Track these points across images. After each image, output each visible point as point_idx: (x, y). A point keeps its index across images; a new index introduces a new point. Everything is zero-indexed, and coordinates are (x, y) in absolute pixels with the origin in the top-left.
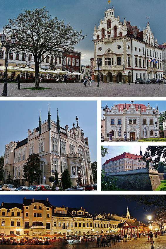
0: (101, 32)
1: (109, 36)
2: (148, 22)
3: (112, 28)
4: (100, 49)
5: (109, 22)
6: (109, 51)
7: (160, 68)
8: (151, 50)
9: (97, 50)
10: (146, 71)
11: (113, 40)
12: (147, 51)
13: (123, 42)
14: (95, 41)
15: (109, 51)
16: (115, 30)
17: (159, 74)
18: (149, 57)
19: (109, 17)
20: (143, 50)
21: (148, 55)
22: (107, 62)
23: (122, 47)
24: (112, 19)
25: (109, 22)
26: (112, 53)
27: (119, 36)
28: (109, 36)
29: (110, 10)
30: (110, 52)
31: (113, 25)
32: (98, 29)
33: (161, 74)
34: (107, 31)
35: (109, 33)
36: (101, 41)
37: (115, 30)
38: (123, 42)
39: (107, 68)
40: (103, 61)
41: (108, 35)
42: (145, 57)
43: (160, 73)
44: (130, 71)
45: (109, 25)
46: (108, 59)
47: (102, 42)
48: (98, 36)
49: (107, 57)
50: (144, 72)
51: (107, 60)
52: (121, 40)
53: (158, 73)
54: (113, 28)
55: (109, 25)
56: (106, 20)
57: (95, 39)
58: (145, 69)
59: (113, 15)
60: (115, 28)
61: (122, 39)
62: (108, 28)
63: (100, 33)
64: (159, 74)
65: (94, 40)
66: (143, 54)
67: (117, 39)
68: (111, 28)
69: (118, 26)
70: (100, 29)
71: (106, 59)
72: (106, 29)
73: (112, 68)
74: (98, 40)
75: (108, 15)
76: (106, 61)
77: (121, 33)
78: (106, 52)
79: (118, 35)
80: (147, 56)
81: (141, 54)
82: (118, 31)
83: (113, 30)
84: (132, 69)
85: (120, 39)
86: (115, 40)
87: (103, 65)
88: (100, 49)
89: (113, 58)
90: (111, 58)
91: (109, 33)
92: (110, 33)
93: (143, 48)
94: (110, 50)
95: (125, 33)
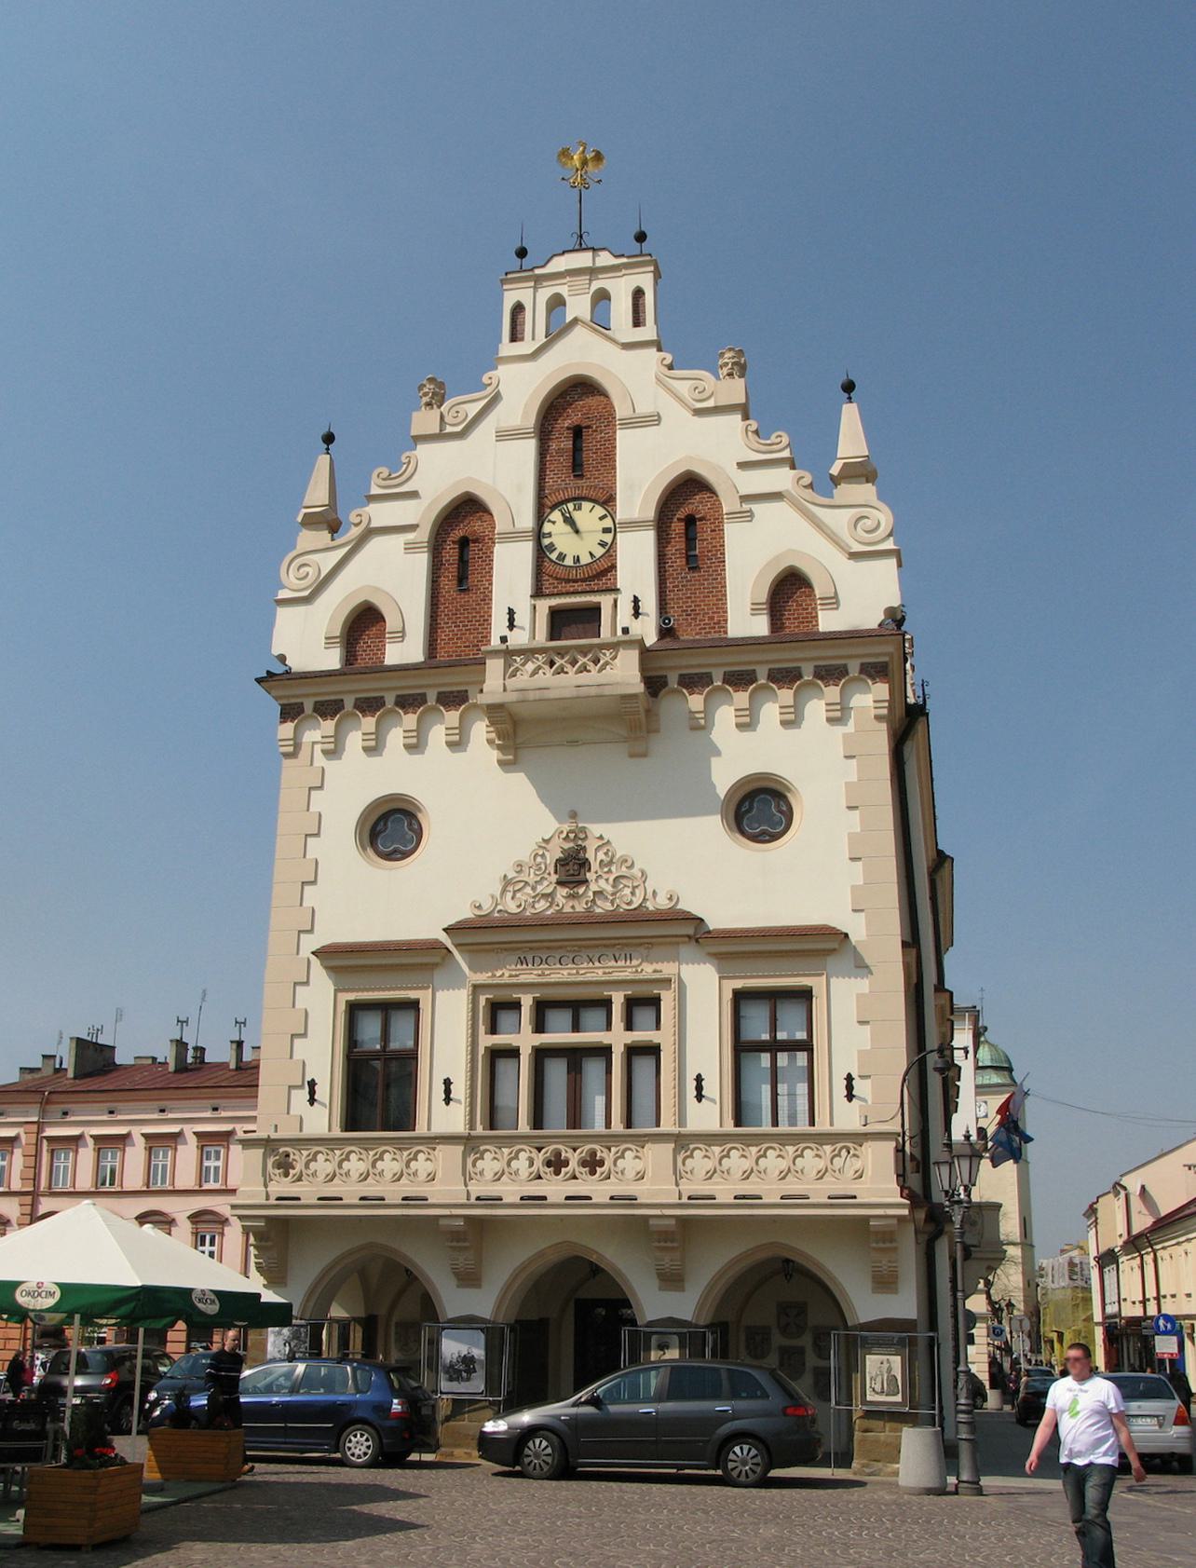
0: (422, 561)
4: (391, 828)
5: (574, 432)
6: (573, 867)
9: (338, 844)
11: (654, 685)
13: (850, 727)
14: (297, 697)
15: (573, 867)
19: (581, 353)
24: (631, 374)
25: (574, 432)
26: (640, 917)
27: (760, 626)
29: (605, 259)
30: (598, 882)
31: (640, 470)
34: (527, 549)
36: (443, 684)
39: (509, 1178)
40: (447, 1037)
45: (577, 467)
49: (527, 977)
51: (526, 1040)
55: (577, 467)
56: (522, 385)
57: (297, 663)
60: (687, 512)
63: (396, 575)
65: (277, 679)
68: (608, 501)
69: (731, 482)
70: (422, 513)
71: (499, 1009)
72: (526, 520)
73: (646, 1179)
74: (359, 684)
75: (558, 329)
82: (746, 559)
83: (648, 538)
85: (784, 677)
87: (443, 1114)
88: (391, 828)
89: (643, 1003)
90: (607, 1004)
92: (602, 573)
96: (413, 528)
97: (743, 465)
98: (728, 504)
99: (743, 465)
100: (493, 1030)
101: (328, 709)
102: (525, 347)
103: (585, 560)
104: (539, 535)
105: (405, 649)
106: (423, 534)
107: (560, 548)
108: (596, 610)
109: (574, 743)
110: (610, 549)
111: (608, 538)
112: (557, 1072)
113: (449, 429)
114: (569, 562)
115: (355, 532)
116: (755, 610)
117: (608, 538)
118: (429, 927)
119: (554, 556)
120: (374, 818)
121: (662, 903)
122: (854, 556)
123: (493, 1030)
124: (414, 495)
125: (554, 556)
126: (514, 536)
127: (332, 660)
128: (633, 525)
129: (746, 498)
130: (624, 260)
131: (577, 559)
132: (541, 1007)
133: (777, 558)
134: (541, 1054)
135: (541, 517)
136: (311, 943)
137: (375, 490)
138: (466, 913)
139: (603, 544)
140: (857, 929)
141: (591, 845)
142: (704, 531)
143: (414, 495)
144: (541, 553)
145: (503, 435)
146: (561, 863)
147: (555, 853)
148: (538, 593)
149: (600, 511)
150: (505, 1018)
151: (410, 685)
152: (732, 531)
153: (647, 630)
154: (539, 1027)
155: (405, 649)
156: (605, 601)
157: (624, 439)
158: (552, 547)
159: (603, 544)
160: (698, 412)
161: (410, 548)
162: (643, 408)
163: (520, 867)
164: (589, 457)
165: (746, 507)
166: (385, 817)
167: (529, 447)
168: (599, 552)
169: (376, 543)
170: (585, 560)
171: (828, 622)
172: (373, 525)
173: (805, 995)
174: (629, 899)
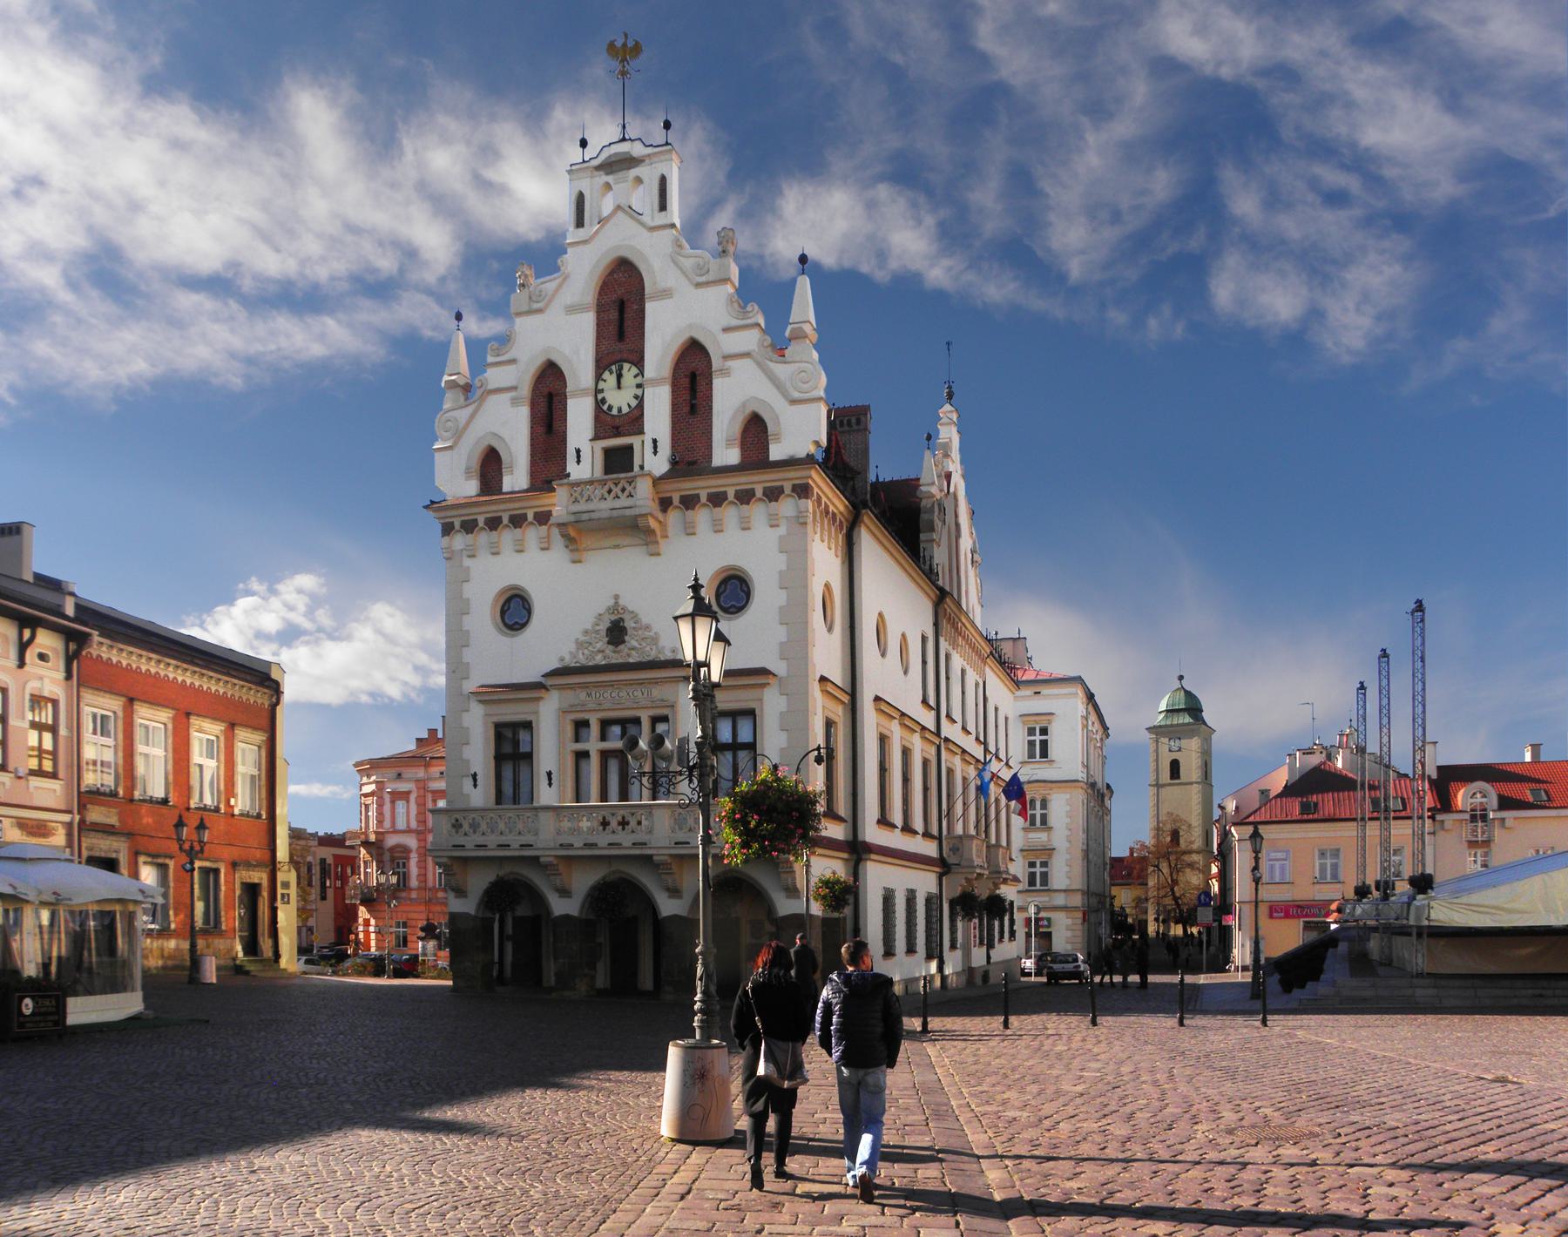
1: (618, 462)
3: (650, 369)
6: (616, 633)
11: (665, 504)
13: (782, 530)
15: (616, 633)
16: (693, 389)
22: (595, 760)
23: (767, 596)
25: (621, 304)
28: (618, 462)
32: (496, 377)
35: (617, 426)
37: (693, 389)
38: (782, 530)
41: (609, 453)
45: (621, 336)
46: (605, 724)
47: (532, 534)
48: (490, 465)
52: (758, 512)
54: (667, 370)
55: (621, 336)
59: (661, 219)
61: (773, 494)
62: (601, 366)
67: (717, 500)
68: (639, 363)
69: (719, 345)
71: (581, 726)
76: (582, 756)
77: (755, 430)
78: (580, 645)
79: (726, 453)
85: (745, 497)
86: (689, 502)
87: (546, 795)
91: (617, 426)
92: (634, 421)
94: (629, 624)
95: (801, 431)
96: (514, 388)
97: (726, 330)
98: (716, 363)
99: (726, 330)
100: (577, 740)
101: (469, 527)
102: (582, 234)
103: (625, 410)
104: (598, 391)
105: (516, 478)
106: (525, 390)
107: (610, 401)
108: (630, 448)
109: (617, 547)
110: (640, 400)
111: (639, 392)
112: (614, 766)
113: (536, 306)
114: (615, 412)
115: (479, 392)
116: (729, 444)
117: (639, 392)
118: (531, 674)
119: (605, 408)
120: (502, 601)
121: (669, 655)
122: (794, 402)
123: (577, 740)
124: (513, 361)
125: (605, 408)
126: (582, 393)
127: (471, 488)
128: (656, 382)
129: (726, 357)
130: (650, 150)
131: (620, 410)
132: (605, 724)
133: (744, 405)
134: (605, 755)
135: (598, 377)
136: (470, 686)
137: (490, 359)
138: (555, 664)
139: (636, 397)
140: (778, 667)
141: (625, 617)
142: (701, 381)
143: (513, 361)
144: (599, 403)
145: (572, 309)
146: (609, 630)
147: (605, 625)
148: (596, 437)
149: (635, 370)
150: (583, 731)
151: (516, 507)
152: (718, 384)
153: (658, 464)
154: (603, 738)
155: (516, 478)
156: (634, 440)
157: (650, 308)
158: (604, 401)
159: (636, 397)
160: (698, 285)
161: (515, 402)
162: (662, 285)
163: (586, 632)
164: (628, 323)
165: (730, 363)
166: (508, 600)
167: (588, 320)
168: (634, 403)
169: (493, 400)
170: (625, 410)
171: (776, 452)
172: (490, 387)
173: (751, 713)
174: (652, 654)
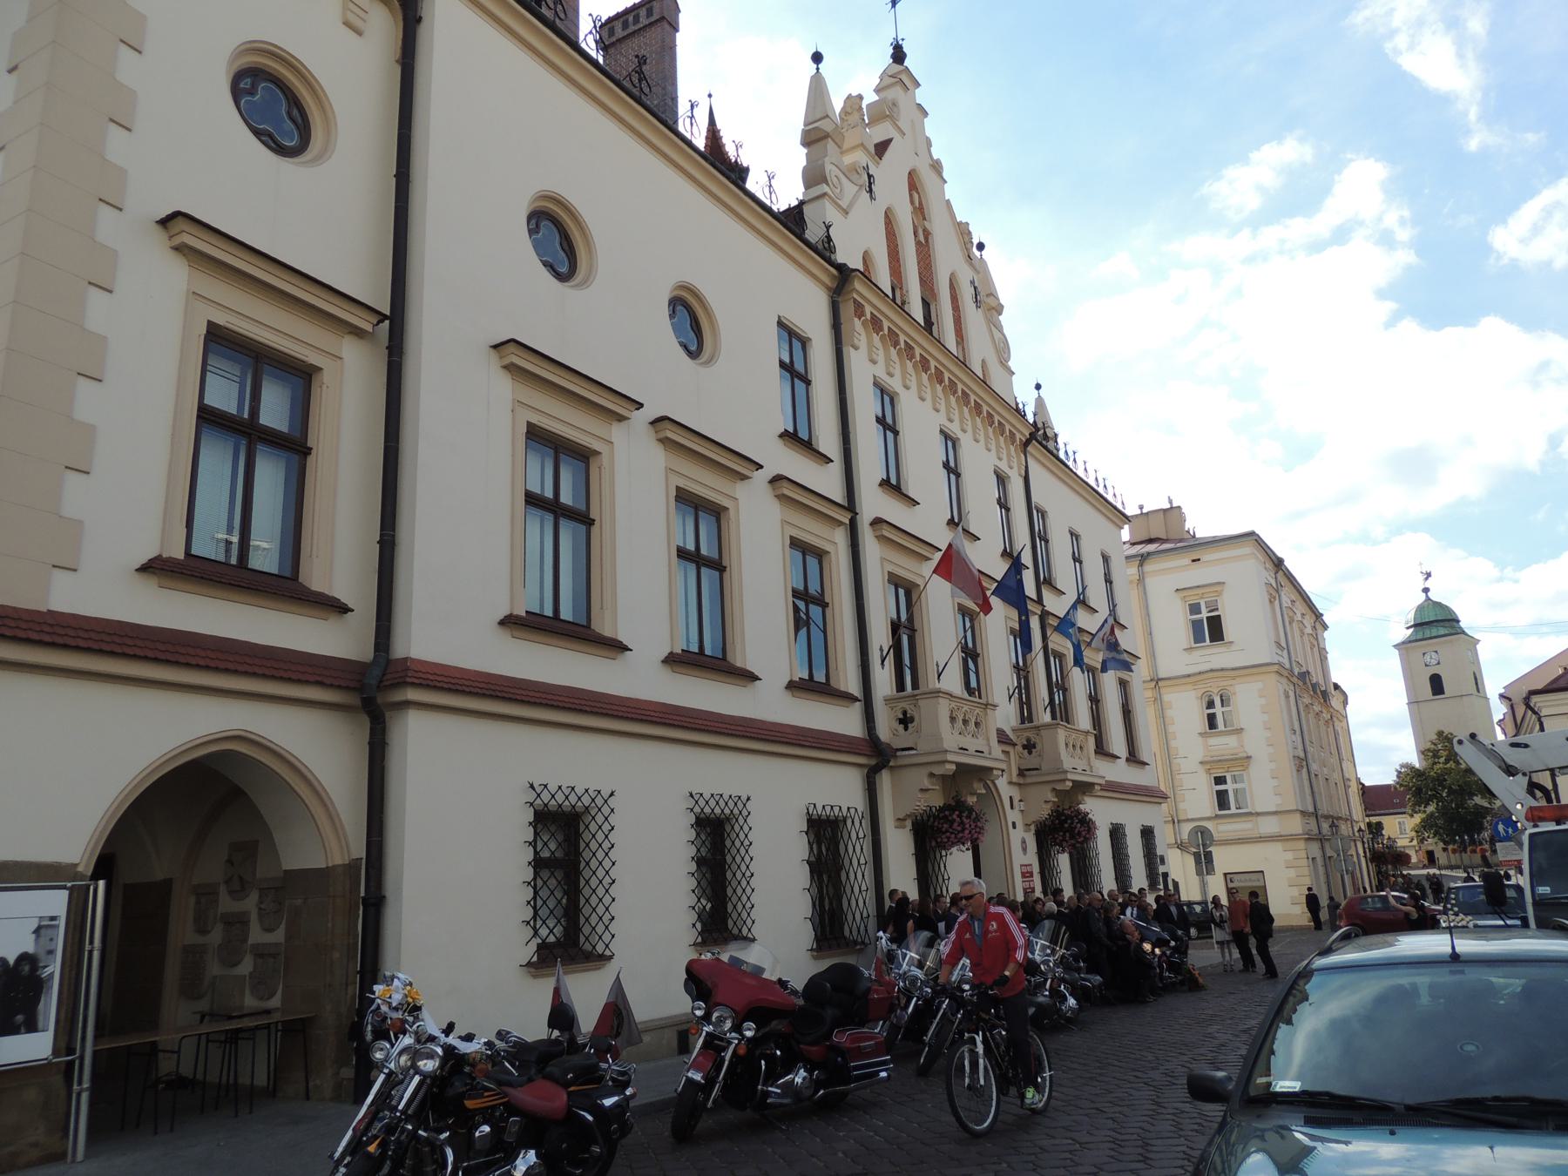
2: (899, 55)
7: (1118, 744)
8: (966, 441)
10: (876, 757)
12: (888, 426)
17: (1117, 833)
18: (929, 522)
20: (795, 373)
21: (892, 486)
33: (1147, 834)
42: (851, 505)
43: (1133, 817)
44: (310, 742)
50: (839, 788)
53: (1101, 812)
58: (845, 721)
64: (1117, 833)
66: (798, 439)
80: (873, 503)
81: (739, 400)
84: (374, 690)
93: (791, 335)
